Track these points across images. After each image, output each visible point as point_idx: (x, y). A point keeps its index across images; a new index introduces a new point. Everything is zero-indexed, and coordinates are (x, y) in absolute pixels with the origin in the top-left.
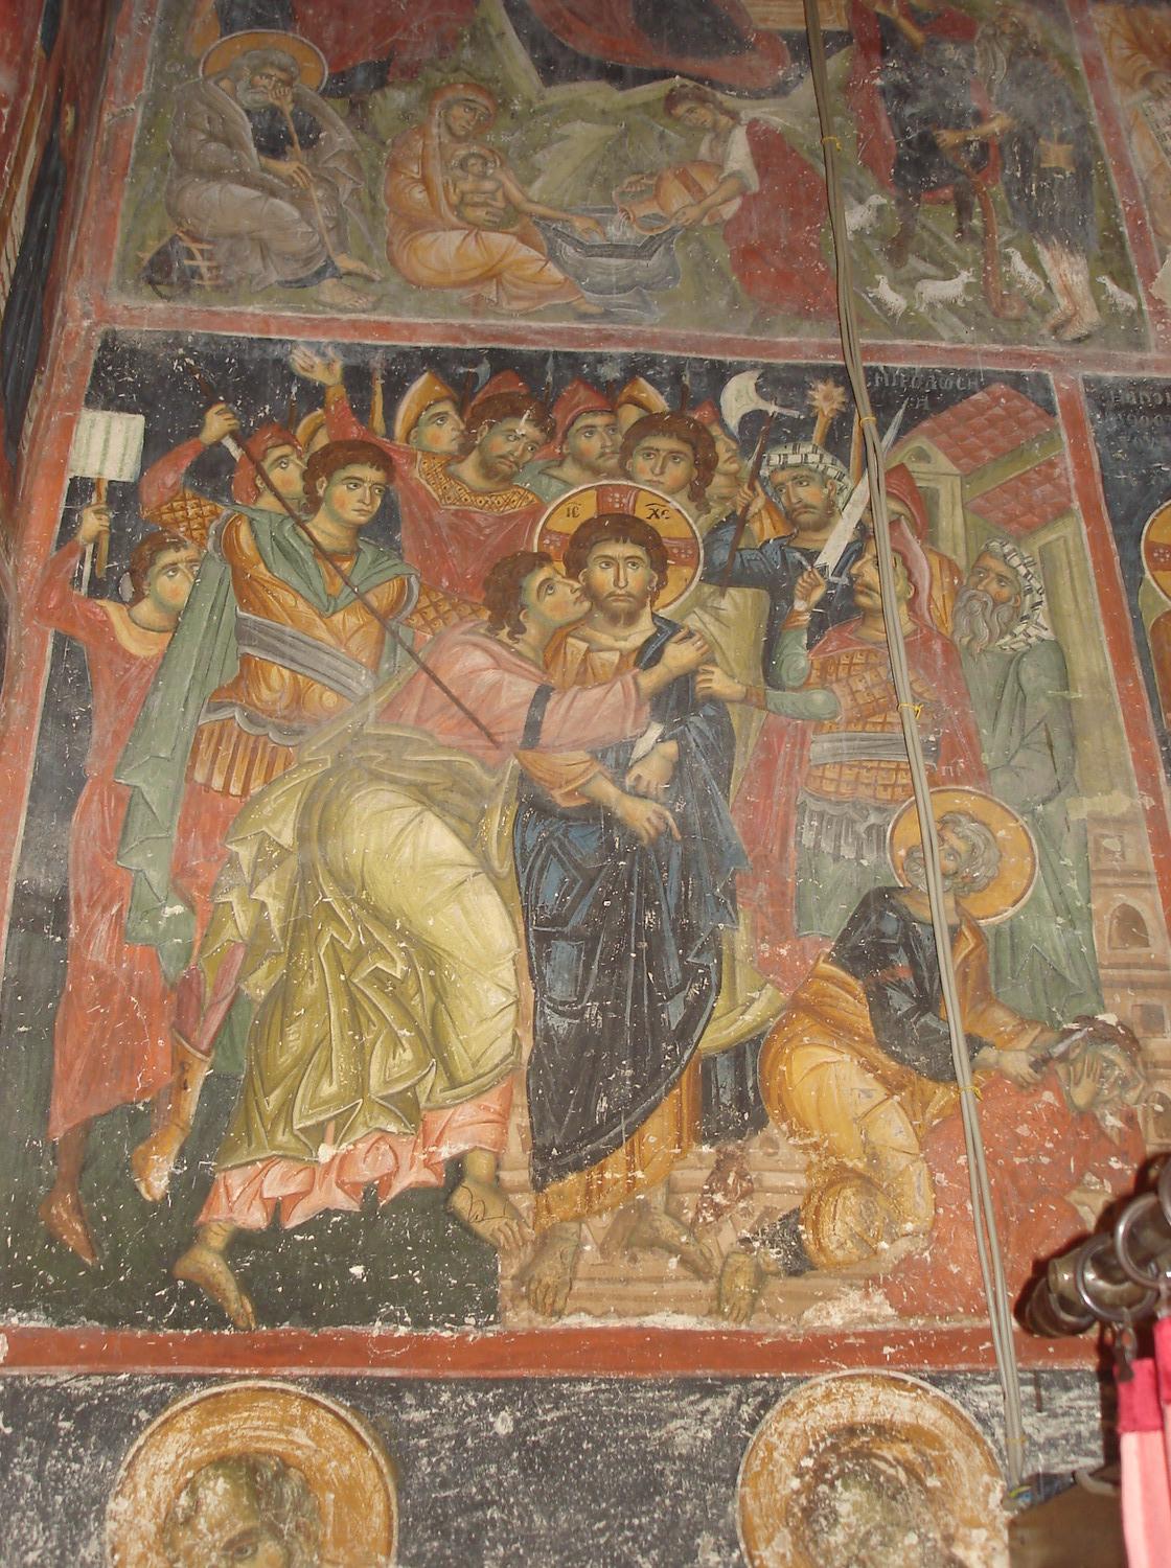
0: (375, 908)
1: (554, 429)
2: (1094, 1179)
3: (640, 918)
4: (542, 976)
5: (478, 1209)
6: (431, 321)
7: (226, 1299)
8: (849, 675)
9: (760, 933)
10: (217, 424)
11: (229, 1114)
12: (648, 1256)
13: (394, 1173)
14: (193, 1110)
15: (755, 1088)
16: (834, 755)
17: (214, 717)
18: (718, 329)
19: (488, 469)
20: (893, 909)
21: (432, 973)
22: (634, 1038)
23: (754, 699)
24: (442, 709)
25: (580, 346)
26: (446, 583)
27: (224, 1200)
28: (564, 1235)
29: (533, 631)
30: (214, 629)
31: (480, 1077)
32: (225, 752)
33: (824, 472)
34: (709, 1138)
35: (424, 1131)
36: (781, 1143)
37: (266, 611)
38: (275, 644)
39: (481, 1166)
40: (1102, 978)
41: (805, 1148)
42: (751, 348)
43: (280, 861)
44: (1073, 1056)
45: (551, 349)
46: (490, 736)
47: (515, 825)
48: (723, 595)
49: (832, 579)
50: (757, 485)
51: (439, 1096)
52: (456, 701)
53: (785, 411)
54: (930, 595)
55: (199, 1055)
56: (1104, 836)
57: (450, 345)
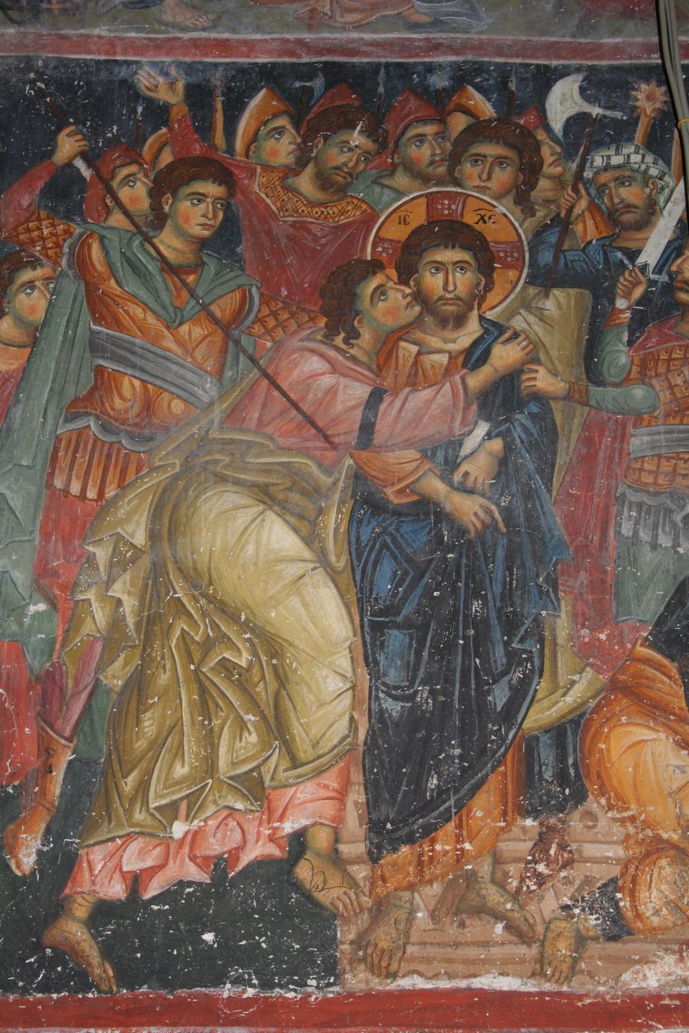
0: (222, 603)
1: (386, 139)
3: (467, 606)
4: (376, 663)
5: (319, 880)
6: (267, 37)
7: (89, 965)
8: (668, 370)
9: (580, 619)
10: (67, 145)
11: (90, 795)
12: (476, 922)
13: (241, 847)
14: (58, 791)
15: (575, 765)
16: (653, 448)
17: (70, 426)
18: (543, 32)
19: (323, 180)
21: (274, 661)
22: (462, 719)
23: (577, 396)
24: (283, 412)
25: (410, 57)
26: (284, 292)
27: (87, 874)
28: (398, 902)
29: (366, 336)
30: (69, 343)
31: (319, 757)
32: (83, 460)
33: (646, 172)
34: (533, 812)
35: (269, 809)
36: (600, 815)
37: (118, 324)
38: (125, 354)
39: (321, 839)
41: (622, 821)
42: (576, 51)
43: (133, 561)
45: (383, 60)
46: (327, 438)
48: (547, 296)
49: (652, 276)
50: (581, 187)
51: (282, 775)
52: (295, 405)
53: (608, 113)
55: (63, 741)
57: (287, 60)
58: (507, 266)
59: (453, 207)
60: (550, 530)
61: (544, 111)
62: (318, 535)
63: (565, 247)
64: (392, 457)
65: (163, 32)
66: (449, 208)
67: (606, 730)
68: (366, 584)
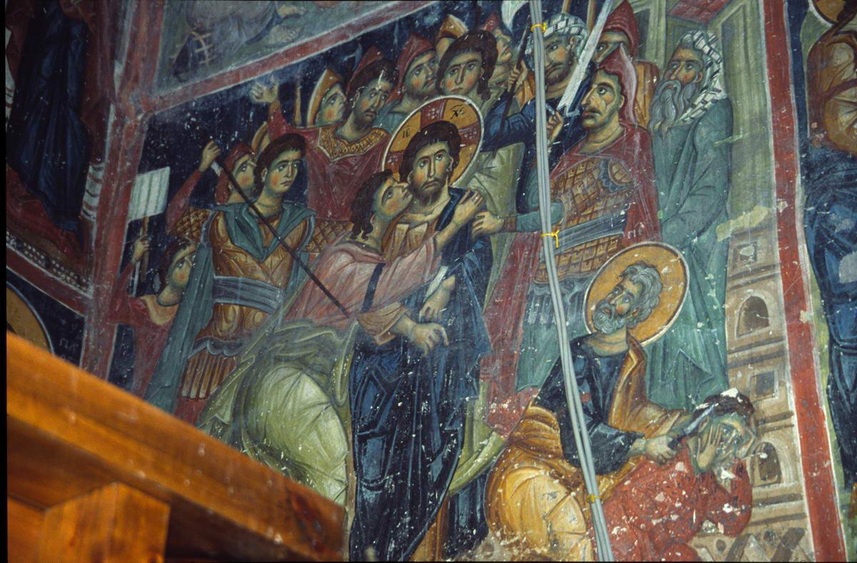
0: (271, 448)
2: (710, 524)
3: (419, 409)
4: (361, 466)
9: (492, 397)
10: (209, 154)
15: (481, 510)
17: (196, 351)
19: (361, 125)
20: (583, 353)
25: (415, 8)
29: (377, 228)
36: (496, 546)
40: (729, 361)
41: (510, 546)
44: (701, 429)
47: (351, 367)
48: (494, 157)
54: (635, 100)
56: (740, 247)
57: (340, 43)
58: (469, 143)
59: (438, 112)
60: (479, 335)
61: (500, 13)
62: (332, 382)
63: (509, 114)
64: (381, 312)
65: (268, 53)
66: (435, 113)
67: (503, 477)
68: (358, 410)
